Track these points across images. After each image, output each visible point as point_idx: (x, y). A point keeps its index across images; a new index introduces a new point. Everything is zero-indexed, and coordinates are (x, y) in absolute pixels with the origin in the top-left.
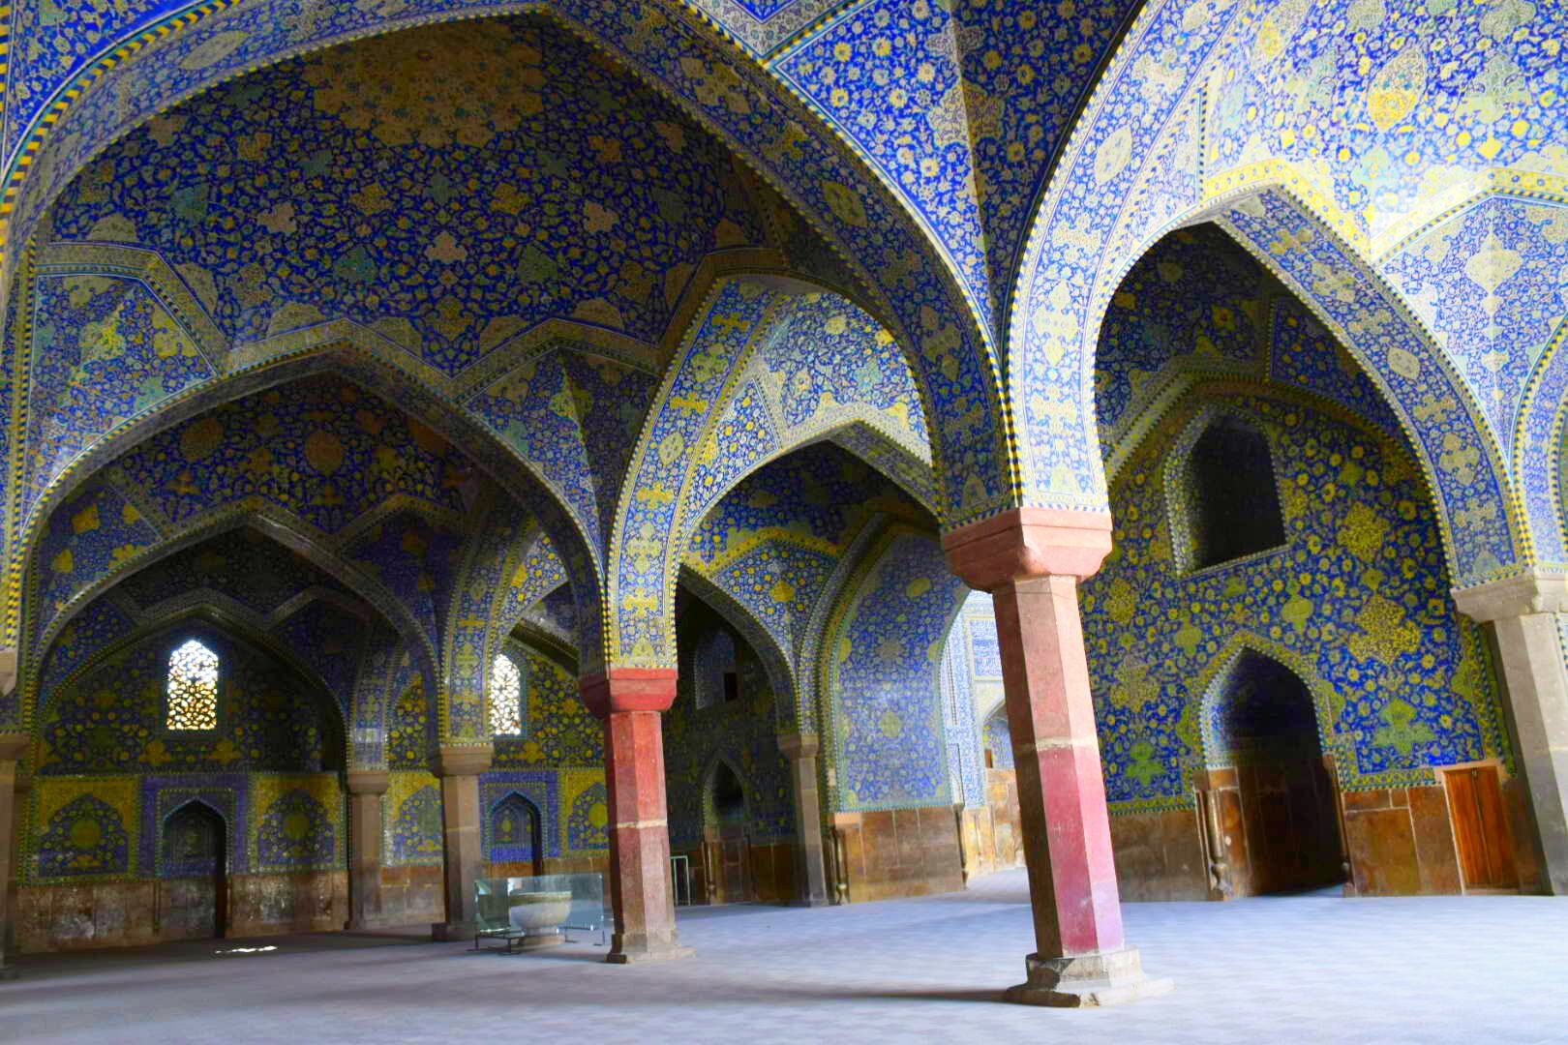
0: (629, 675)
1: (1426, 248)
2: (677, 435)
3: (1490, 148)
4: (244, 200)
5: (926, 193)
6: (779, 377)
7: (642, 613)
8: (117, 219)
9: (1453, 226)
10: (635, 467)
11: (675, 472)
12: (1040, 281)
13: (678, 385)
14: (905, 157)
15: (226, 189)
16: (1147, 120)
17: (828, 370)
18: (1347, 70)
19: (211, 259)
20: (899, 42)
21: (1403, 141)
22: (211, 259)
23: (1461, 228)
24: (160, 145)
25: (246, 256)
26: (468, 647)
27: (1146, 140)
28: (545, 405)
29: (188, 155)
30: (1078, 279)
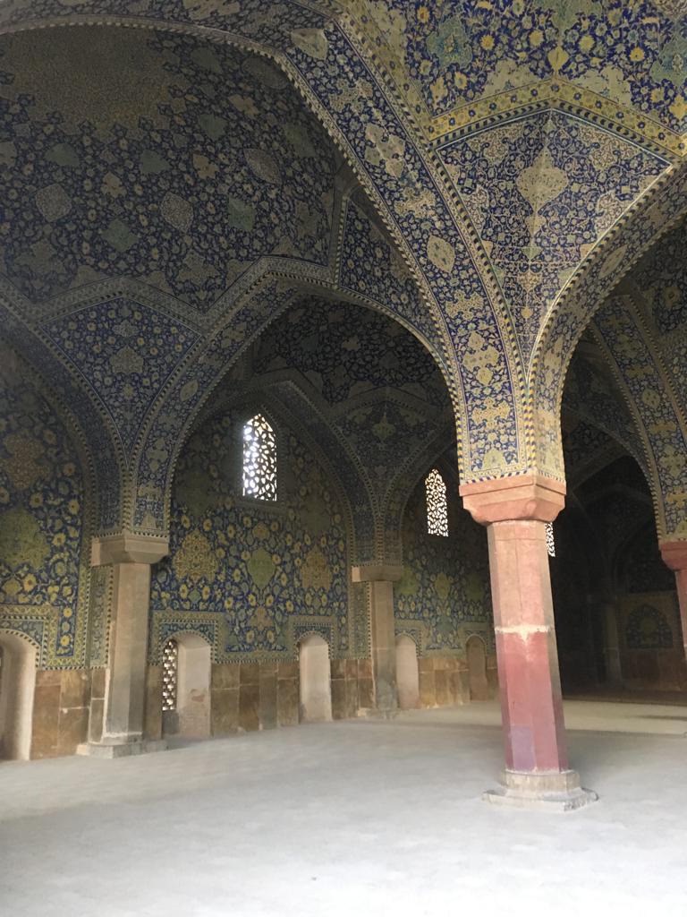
0: (671, 547)
2: (647, 390)
4: (411, 349)
5: (409, 313)
10: (637, 416)
11: (665, 411)
12: (457, 340)
14: (394, 299)
15: (400, 349)
16: (438, 225)
19: (415, 378)
20: (363, 245)
22: (415, 378)
24: (356, 350)
25: (430, 369)
27: (451, 233)
29: (371, 347)
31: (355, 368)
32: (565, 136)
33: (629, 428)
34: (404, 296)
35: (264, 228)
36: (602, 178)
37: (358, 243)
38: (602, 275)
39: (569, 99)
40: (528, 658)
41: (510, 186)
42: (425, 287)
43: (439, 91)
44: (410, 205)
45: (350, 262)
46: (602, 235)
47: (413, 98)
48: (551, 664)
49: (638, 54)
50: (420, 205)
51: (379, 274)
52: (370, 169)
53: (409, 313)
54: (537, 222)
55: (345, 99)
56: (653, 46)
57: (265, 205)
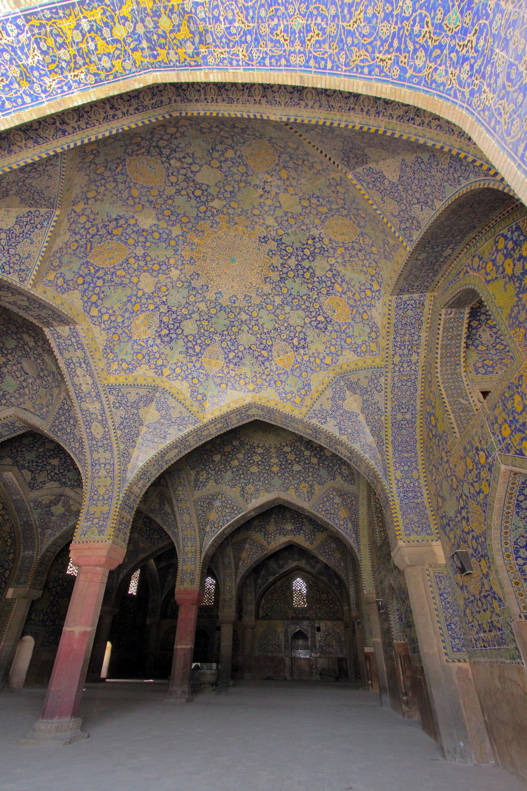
1: (321, 405)
3: (328, 360)
5: (77, 452)
6: (237, 489)
7: (189, 571)
8: (52, 482)
9: (329, 393)
10: (179, 525)
13: (177, 500)
16: (99, 417)
17: (260, 483)
18: (260, 358)
21: (298, 370)
23: (332, 393)
26: (228, 579)
28: (163, 509)
30: (108, 467)
31: (52, 474)
32: (163, 400)
33: (176, 531)
34: (77, 444)
35: (20, 394)
36: (173, 420)
37: (64, 414)
38: (166, 458)
39: (167, 387)
40: (75, 646)
41: (136, 411)
42: (86, 443)
43: (115, 366)
44: (88, 405)
45: (57, 422)
46: (168, 442)
47: (102, 364)
48: (87, 651)
49: (195, 381)
50: (94, 407)
51: (69, 431)
52: (74, 384)
53: (77, 452)
54: (144, 429)
55: (71, 355)
56: (201, 380)
57: (24, 384)
